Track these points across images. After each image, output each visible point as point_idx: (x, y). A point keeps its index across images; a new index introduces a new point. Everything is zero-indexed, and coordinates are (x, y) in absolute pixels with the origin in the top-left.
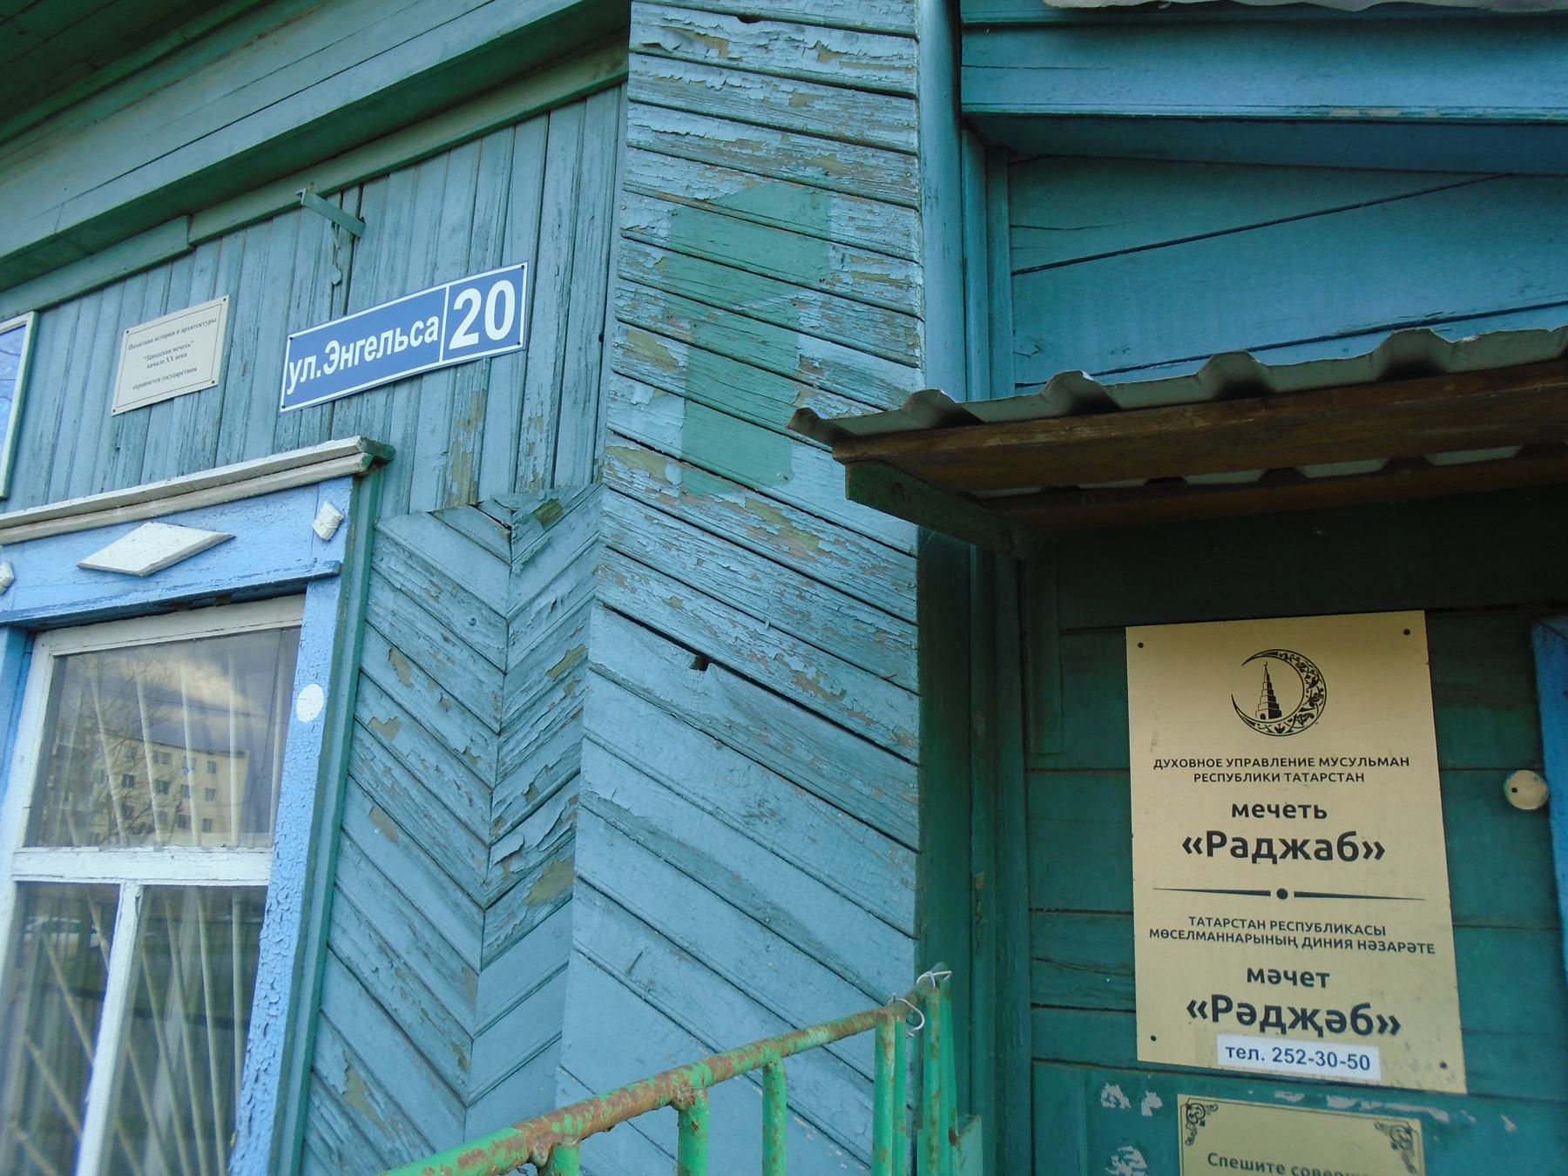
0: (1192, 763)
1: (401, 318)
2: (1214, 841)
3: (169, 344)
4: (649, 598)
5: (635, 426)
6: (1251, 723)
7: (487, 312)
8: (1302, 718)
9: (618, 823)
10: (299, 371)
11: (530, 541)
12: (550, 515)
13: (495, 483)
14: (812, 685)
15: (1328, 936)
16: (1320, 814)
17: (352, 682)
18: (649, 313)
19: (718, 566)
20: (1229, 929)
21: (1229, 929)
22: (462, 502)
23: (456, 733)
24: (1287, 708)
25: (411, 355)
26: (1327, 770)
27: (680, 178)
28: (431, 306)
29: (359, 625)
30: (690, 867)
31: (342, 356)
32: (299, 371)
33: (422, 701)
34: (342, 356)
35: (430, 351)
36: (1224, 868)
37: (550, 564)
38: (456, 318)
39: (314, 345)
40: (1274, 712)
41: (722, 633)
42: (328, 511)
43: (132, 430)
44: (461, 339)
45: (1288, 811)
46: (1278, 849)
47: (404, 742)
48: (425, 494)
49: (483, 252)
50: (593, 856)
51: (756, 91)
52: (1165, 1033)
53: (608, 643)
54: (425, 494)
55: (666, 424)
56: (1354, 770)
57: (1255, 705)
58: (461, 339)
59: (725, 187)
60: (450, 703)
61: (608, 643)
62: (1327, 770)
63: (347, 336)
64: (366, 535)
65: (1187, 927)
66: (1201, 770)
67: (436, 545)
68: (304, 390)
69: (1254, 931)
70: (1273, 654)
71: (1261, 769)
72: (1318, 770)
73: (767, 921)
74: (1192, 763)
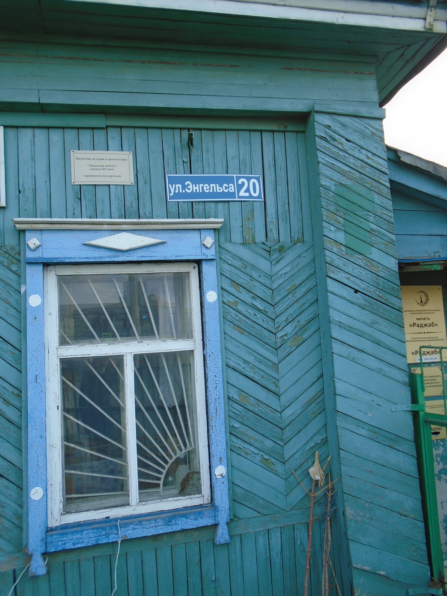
0: (410, 311)
1: (220, 181)
2: (414, 324)
3: (105, 165)
4: (341, 277)
5: (332, 235)
6: (419, 304)
7: (249, 187)
8: (425, 303)
9: (341, 325)
10: (173, 189)
11: (276, 256)
12: (281, 250)
14: (380, 297)
15: (431, 339)
16: (429, 319)
18: (332, 208)
19: (357, 271)
20: (417, 340)
21: (417, 340)
24: (424, 302)
25: (223, 194)
26: (429, 312)
27: (337, 176)
28: (230, 180)
30: (360, 334)
31: (192, 188)
32: (173, 189)
33: (247, 297)
34: (192, 188)
35: (232, 195)
36: (416, 329)
37: (283, 263)
38: (240, 187)
39: (182, 181)
40: (422, 302)
41: (361, 286)
44: (242, 193)
45: (425, 319)
46: (424, 325)
47: (241, 307)
48: (237, 237)
49: (244, 168)
50: (336, 332)
51: (352, 160)
54: (237, 237)
55: (340, 237)
56: (433, 312)
57: (419, 301)
58: (242, 193)
59: (349, 183)
60: (256, 297)
62: (429, 312)
63: (196, 181)
65: (411, 340)
66: (411, 312)
67: (244, 253)
68: (176, 195)
69: (420, 340)
70: (421, 292)
71: (421, 312)
72: (428, 312)
73: (378, 343)
74: (410, 311)
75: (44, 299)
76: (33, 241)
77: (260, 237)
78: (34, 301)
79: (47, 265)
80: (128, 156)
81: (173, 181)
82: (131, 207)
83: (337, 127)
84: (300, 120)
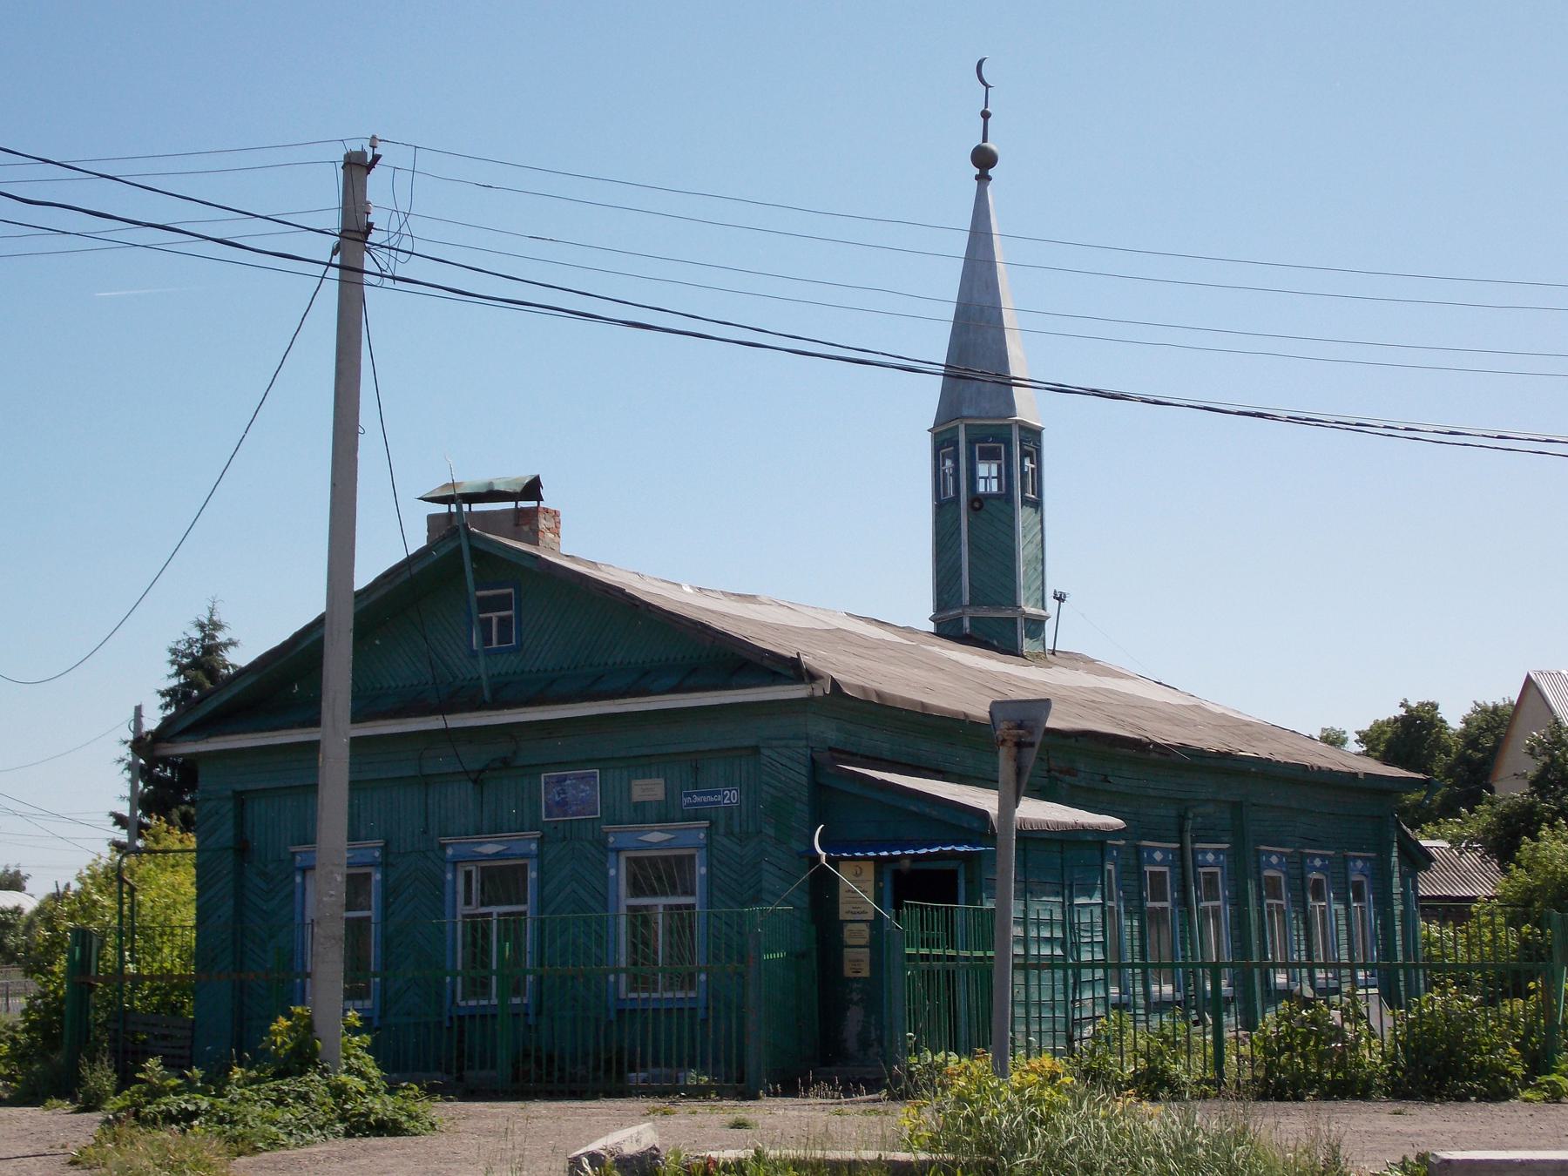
1: (712, 794)
3: (649, 789)
7: (731, 797)
13: (737, 830)
17: (710, 866)
22: (729, 833)
23: (734, 876)
27: (772, 791)
28: (718, 793)
29: (710, 855)
31: (697, 799)
34: (697, 799)
42: (702, 835)
43: (640, 807)
52: (843, 916)
53: (766, 866)
54: (722, 830)
55: (771, 832)
61: (766, 866)
63: (699, 794)
64: (709, 836)
67: (726, 841)
75: (619, 873)
76: (611, 839)
77: (737, 830)
78: (612, 872)
79: (618, 851)
80: (661, 781)
81: (687, 795)
82: (663, 814)
83: (775, 756)
84: (756, 750)
